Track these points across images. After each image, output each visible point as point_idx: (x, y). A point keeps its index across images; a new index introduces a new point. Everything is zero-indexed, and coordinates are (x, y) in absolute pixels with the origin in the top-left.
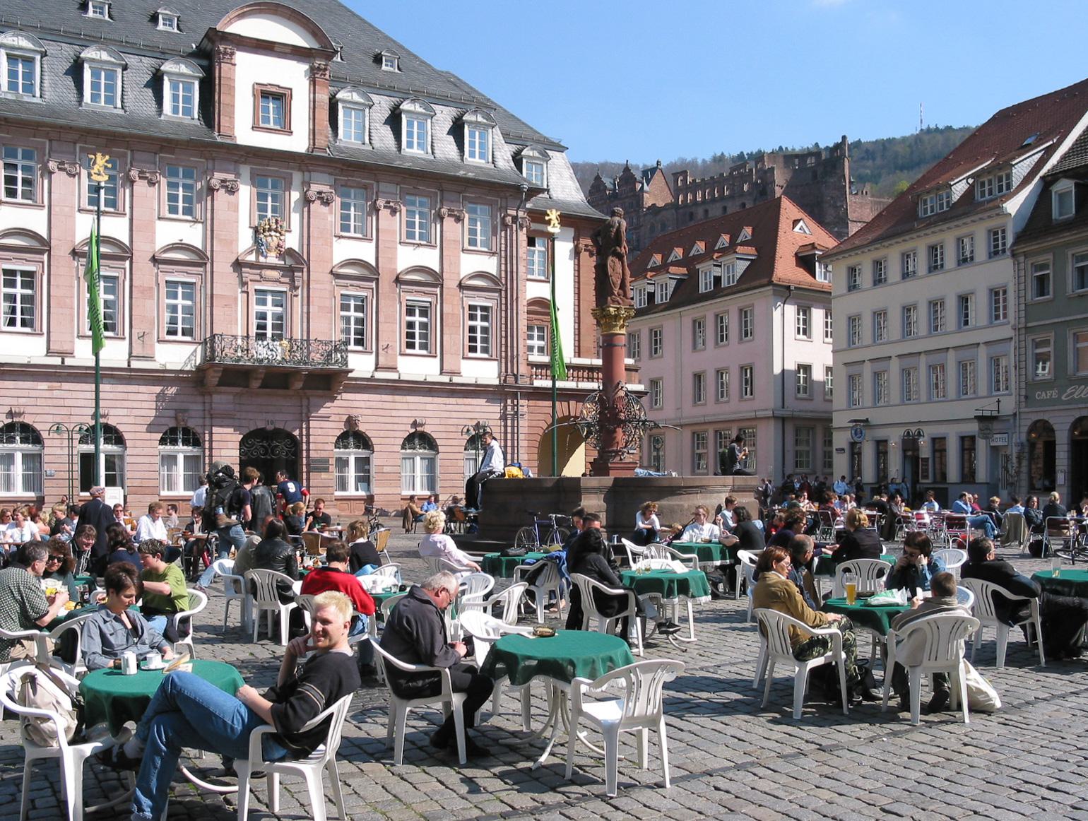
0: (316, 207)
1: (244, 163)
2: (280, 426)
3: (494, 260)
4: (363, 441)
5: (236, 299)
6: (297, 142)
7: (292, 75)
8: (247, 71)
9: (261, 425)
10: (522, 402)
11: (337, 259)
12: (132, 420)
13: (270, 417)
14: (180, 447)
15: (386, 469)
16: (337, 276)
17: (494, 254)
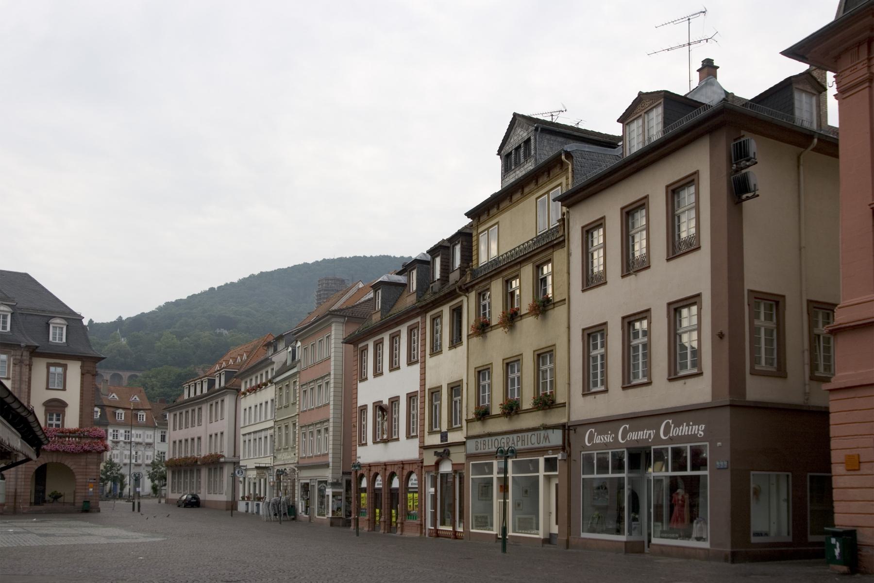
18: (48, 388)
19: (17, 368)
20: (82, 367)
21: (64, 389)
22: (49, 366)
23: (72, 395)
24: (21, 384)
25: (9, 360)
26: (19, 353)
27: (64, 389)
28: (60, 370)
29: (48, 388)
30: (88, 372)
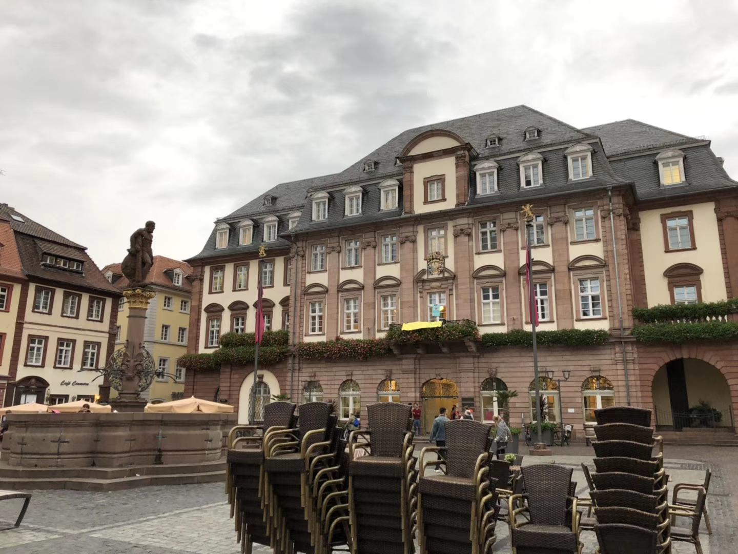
1: (419, 224)
4: (501, 385)
5: (415, 302)
6: (450, 204)
7: (447, 167)
10: (629, 348)
11: (477, 265)
12: (362, 377)
15: (518, 405)
17: (597, 240)
18: (667, 251)
20: (716, 211)
21: (694, 248)
22: (664, 218)
23: (708, 254)
25: (596, 214)
26: (606, 201)
27: (694, 248)
28: (684, 222)
29: (667, 251)
30: (729, 215)
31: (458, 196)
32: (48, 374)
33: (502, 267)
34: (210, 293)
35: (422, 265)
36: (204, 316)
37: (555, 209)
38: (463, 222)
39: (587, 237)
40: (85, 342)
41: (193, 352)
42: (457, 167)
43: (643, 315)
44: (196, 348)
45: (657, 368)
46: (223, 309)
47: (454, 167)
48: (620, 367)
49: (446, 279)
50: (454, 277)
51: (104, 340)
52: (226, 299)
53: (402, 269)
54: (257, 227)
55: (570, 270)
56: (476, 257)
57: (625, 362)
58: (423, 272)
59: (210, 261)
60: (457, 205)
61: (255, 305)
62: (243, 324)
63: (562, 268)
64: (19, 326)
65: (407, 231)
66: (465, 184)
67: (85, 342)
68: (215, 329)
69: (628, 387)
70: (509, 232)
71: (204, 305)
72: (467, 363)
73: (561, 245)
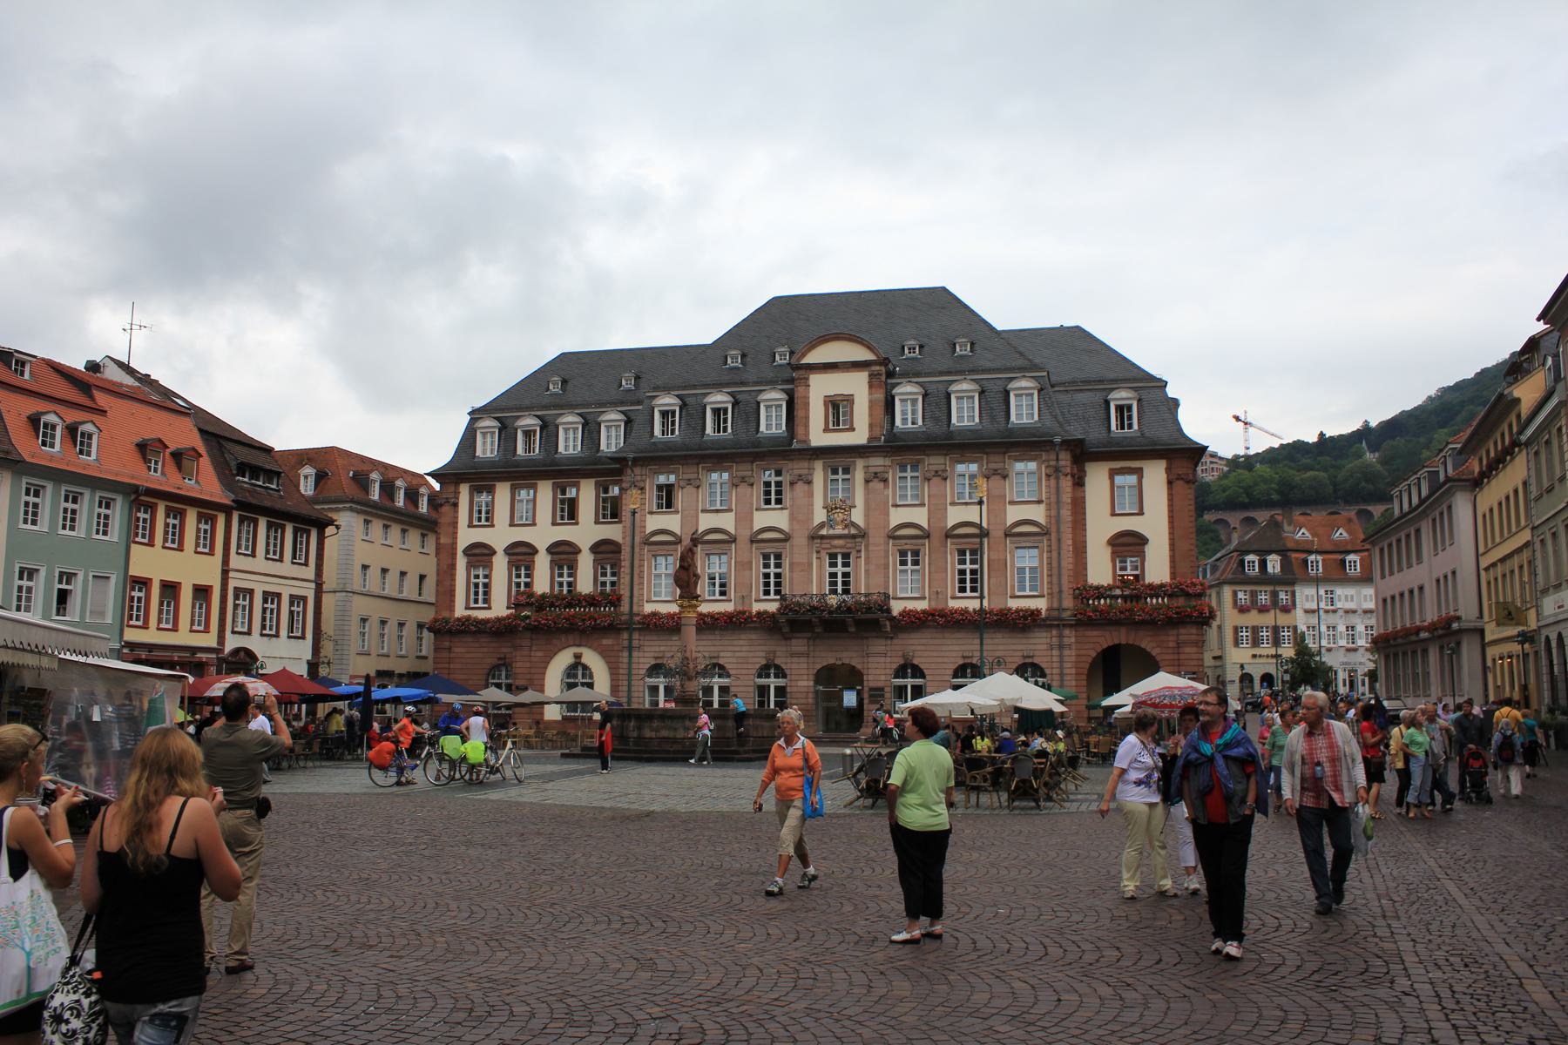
0: (878, 485)
2: (846, 661)
3: (1042, 507)
5: (810, 565)
6: (859, 437)
7: (856, 385)
8: (820, 388)
9: (832, 661)
10: (1067, 632)
11: (893, 523)
13: (839, 655)
14: (772, 679)
16: (895, 538)
17: (1040, 502)
18: (1113, 514)
19: (1053, 482)
20: (1168, 470)
21: (1141, 513)
22: (1113, 473)
23: (1155, 523)
24: (1058, 509)
25: (1039, 468)
27: (1141, 513)
28: (1132, 479)
31: (871, 426)
32: (255, 644)
33: (925, 526)
34: (471, 525)
35: (820, 516)
36: (461, 562)
37: (992, 458)
38: (877, 462)
39: (1025, 494)
40: (291, 596)
41: (445, 614)
42: (871, 386)
43: (1085, 593)
44: (452, 608)
45: (1094, 654)
46: (494, 552)
47: (867, 386)
48: (1055, 652)
49: (854, 537)
50: (863, 535)
51: (309, 592)
52: (500, 536)
53: (792, 518)
54: (549, 429)
55: (1006, 535)
56: (892, 510)
57: (1061, 647)
58: (822, 525)
59: (466, 472)
60: (870, 439)
61: (550, 550)
62: (527, 576)
63: (997, 533)
64: (225, 573)
65: (799, 467)
66: (880, 411)
67: (291, 596)
68: (481, 580)
69: (1061, 675)
70: (936, 480)
71: (462, 544)
72: (878, 646)
73: (998, 502)
